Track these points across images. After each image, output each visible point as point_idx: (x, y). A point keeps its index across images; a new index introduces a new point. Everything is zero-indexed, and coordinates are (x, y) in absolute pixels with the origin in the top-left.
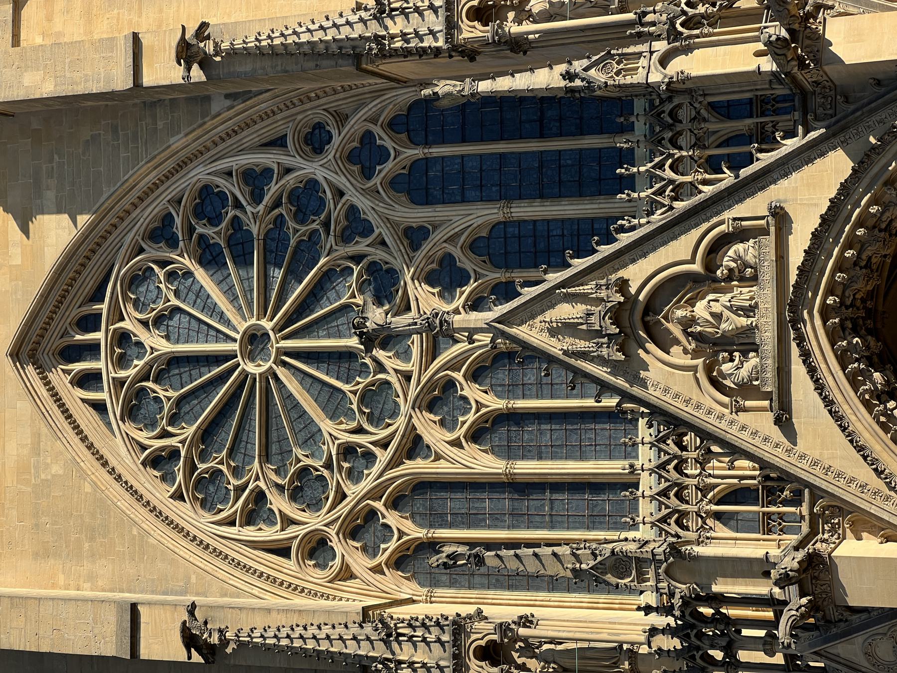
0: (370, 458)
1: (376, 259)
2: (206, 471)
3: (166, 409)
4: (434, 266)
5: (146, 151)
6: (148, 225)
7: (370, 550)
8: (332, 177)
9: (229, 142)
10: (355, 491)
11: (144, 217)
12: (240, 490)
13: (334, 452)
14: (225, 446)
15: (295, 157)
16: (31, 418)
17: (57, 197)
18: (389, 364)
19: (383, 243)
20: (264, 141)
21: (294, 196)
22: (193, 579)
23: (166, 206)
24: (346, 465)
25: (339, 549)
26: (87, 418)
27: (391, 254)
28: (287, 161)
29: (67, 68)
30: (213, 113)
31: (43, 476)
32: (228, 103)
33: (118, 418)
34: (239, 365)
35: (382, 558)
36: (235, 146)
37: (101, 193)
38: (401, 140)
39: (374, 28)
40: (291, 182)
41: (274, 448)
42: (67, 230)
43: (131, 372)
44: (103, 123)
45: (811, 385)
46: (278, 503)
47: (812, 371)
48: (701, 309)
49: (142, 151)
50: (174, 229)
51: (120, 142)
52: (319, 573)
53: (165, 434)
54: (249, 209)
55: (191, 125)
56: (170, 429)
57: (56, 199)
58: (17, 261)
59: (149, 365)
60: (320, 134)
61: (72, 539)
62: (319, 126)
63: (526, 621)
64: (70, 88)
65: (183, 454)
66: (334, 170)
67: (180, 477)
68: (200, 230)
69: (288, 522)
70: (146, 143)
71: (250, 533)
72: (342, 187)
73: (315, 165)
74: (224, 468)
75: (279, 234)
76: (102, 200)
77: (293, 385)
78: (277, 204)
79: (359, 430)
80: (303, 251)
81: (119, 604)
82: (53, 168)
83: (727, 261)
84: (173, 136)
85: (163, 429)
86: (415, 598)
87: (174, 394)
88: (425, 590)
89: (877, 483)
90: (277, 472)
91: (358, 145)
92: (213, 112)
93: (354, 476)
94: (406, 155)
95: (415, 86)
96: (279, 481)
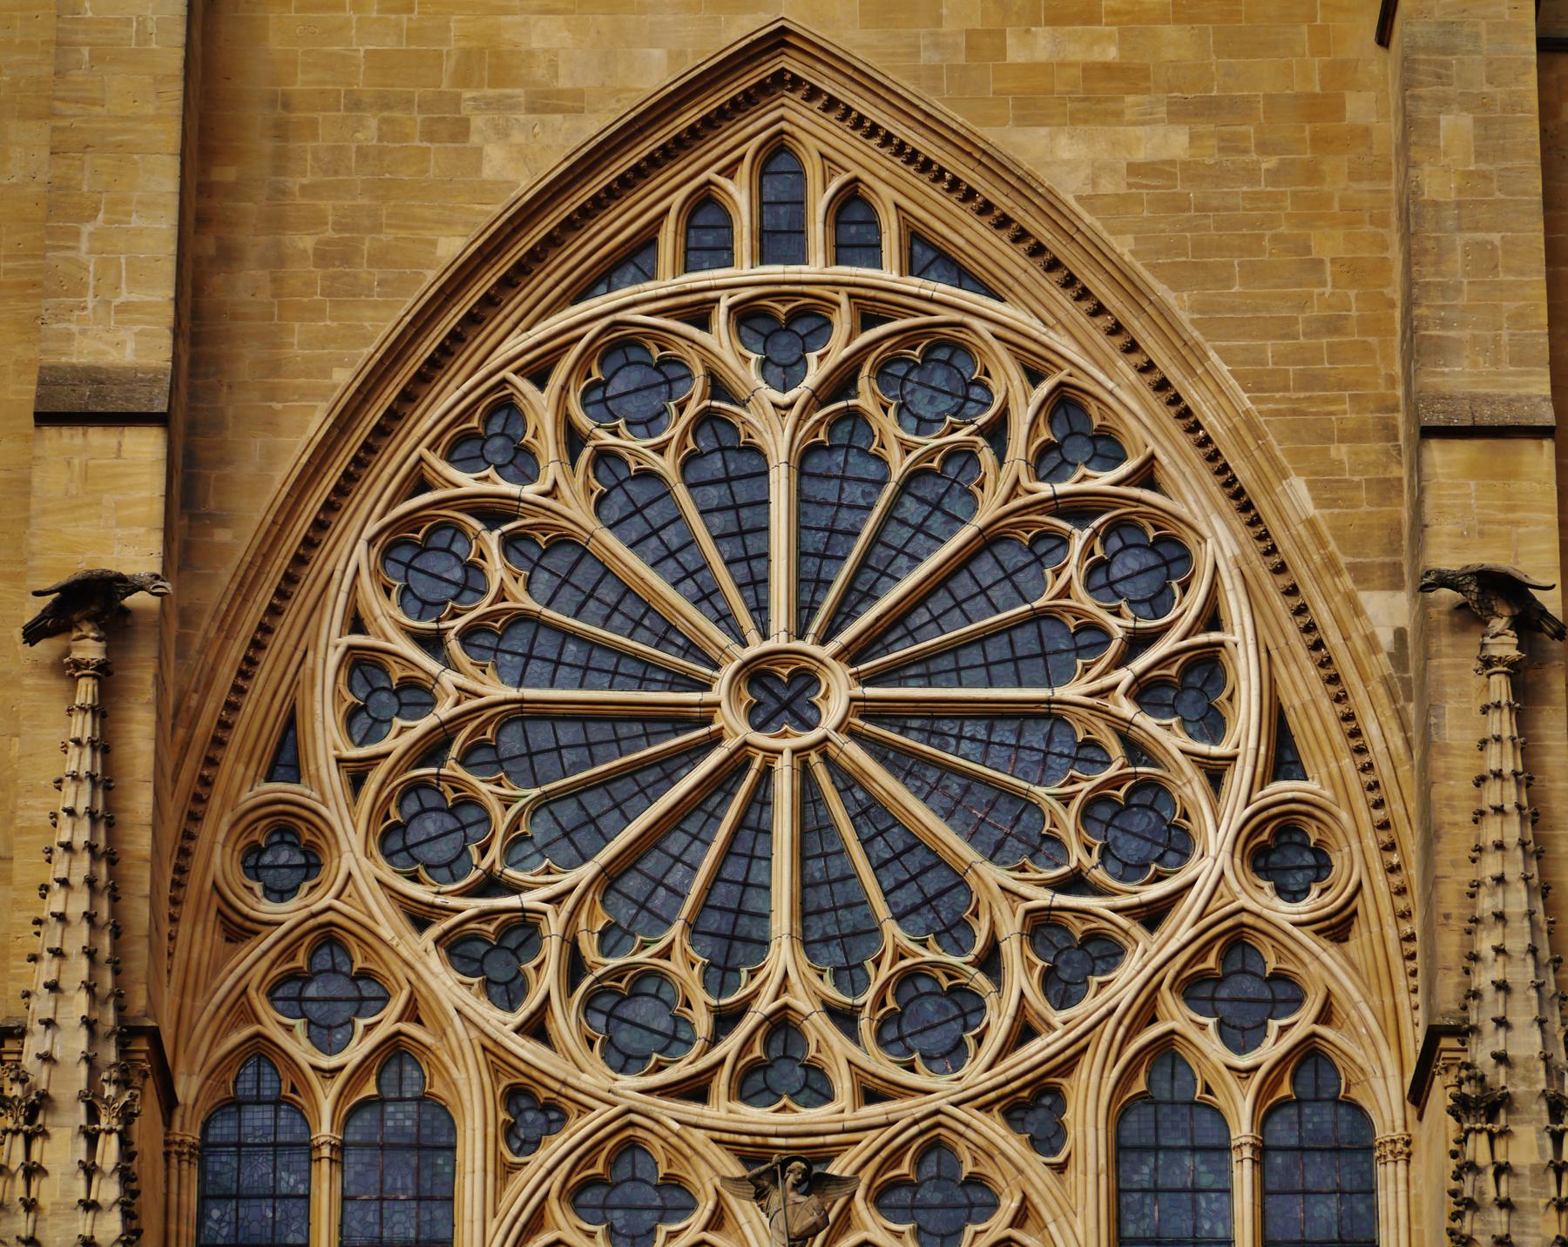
0: (508, 992)
1: (991, 1015)
4: (968, 1168)
5: (1278, 413)
6: (1097, 399)
8: (1192, 904)
9: (1291, 627)
11: (1117, 391)
13: (529, 900)
14: (548, 605)
15: (1248, 804)
16: (620, 91)
17: (1172, 163)
18: (731, 1043)
19: (1023, 1031)
20: (1292, 719)
21: (1152, 792)
22: (223, 535)
23: (1141, 446)
25: (289, 912)
26: (618, 225)
27: (1002, 1054)
28: (1239, 779)
29: (1479, 236)
30: (1363, 596)
31: (478, 121)
32: (1386, 638)
33: (619, 316)
34: (744, 644)
35: (271, 1023)
36: (1282, 642)
37: (1176, 286)
38: (1278, 1082)
40: (1188, 790)
41: (541, 735)
42: (1088, 190)
44: (1352, 293)
49: (1276, 401)
50: (1083, 470)
51: (1302, 340)
53: (573, 440)
54: (1124, 676)
55: (1336, 538)
56: (586, 453)
57: (1165, 162)
58: (1016, 53)
60: (1301, 868)
61: (322, 204)
62: (1322, 866)
64: (1430, 244)
65: (529, 492)
66: (1211, 907)
67: (467, 483)
68: (1079, 539)
70: (1294, 412)
72: (1168, 926)
73: (1224, 858)
75: (1061, 755)
76: (1161, 290)
78: (1136, 749)
79: (575, 967)
80: (1018, 819)
82: (1246, 151)
84: (1311, 485)
85: (589, 437)
86: (178, 1113)
91: (1269, 969)
92: (1363, 596)
94: (1238, 1097)
95: (1406, 1127)
96: (454, 751)
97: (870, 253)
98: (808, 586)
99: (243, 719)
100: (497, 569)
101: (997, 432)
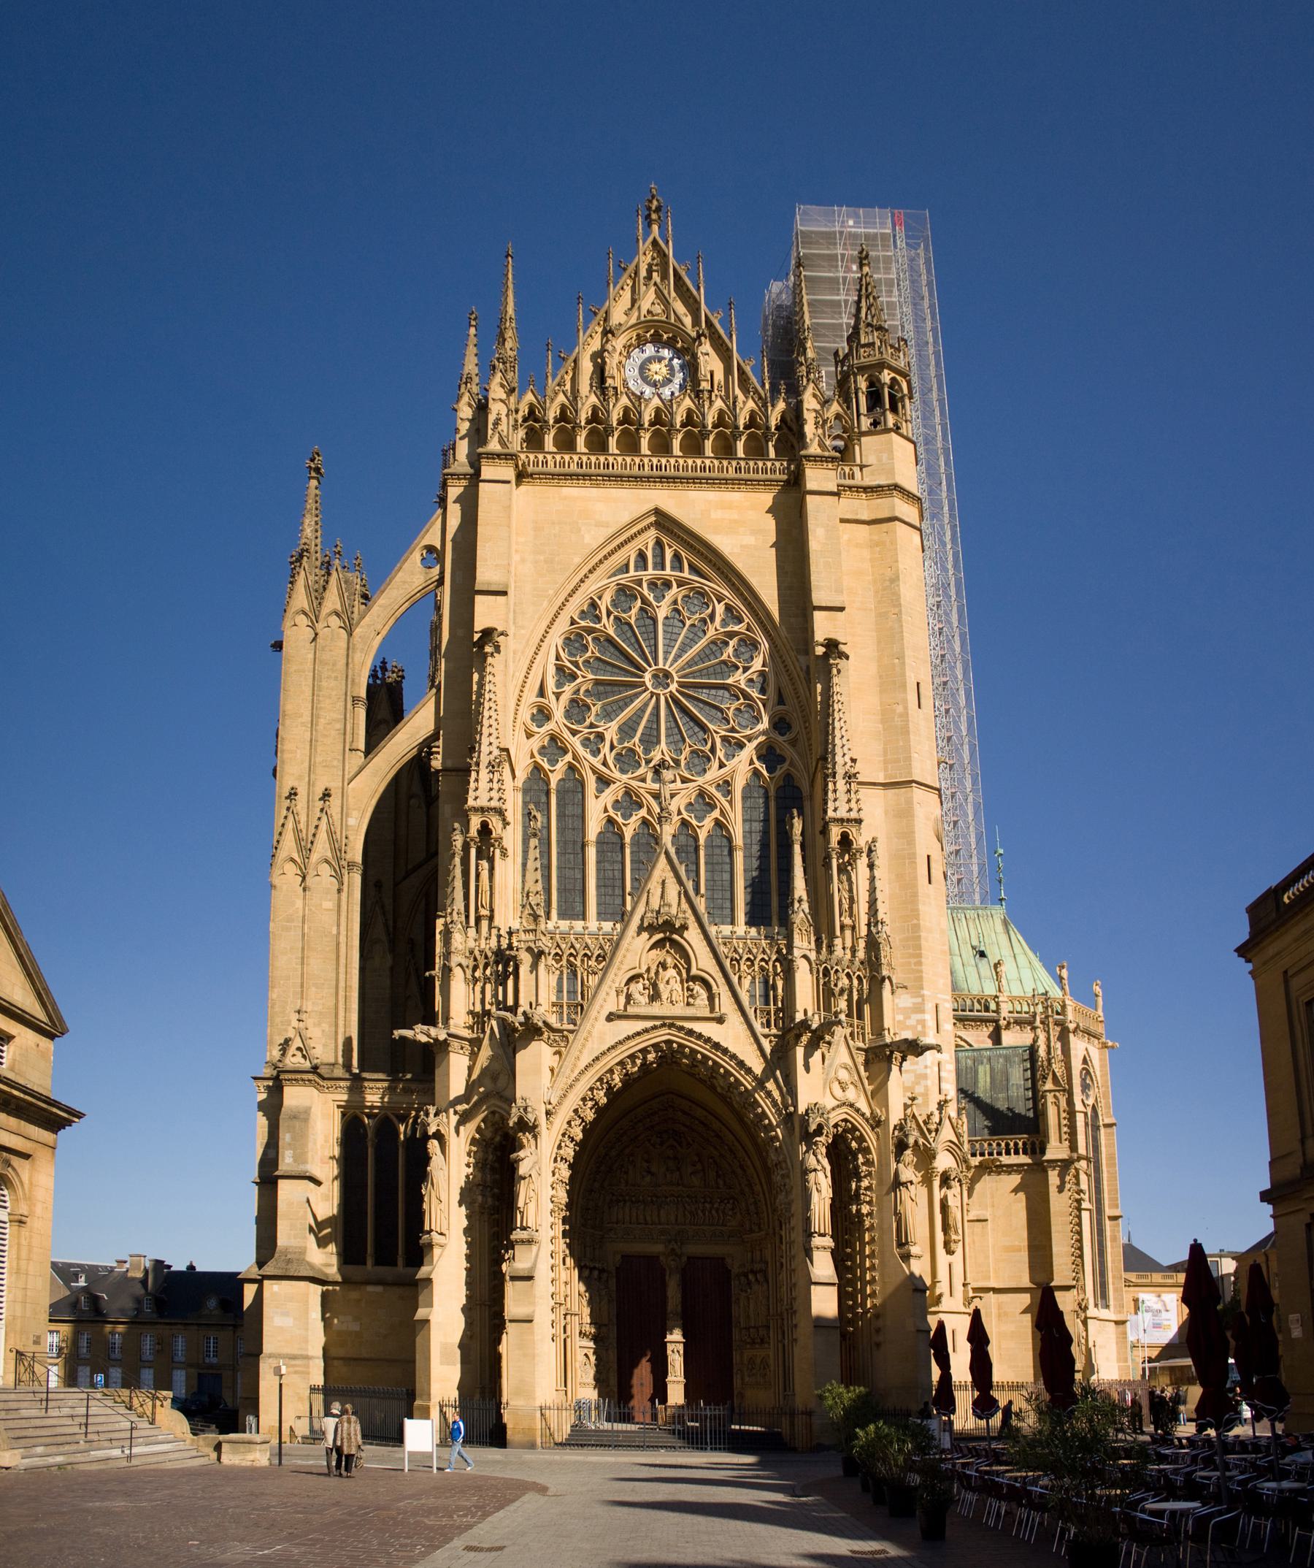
2: (587, 642)
3: (624, 615)
7: (542, 750)
10: (576, 742)
12: (577, 666)
13: (599, 730)
24: (592, 737)
25: (542, 730)
34: (650, 666)
35: (538, 758)
39: (840, 771)
41: (601, 688)
43: (646, 592)
45: (630, 1034)
46: (568, 689)
47: (638, 1034)
48: (671, 972)
52: (529, 717)
56: (612, 617)
59: (650, 605)
63: (504, 854)
65: (597, 626)
69: (558, 696)
71: (551, 670)
74: (589, 654)
77: (637, 703)
81: (507, 586)
83: (698, 988)
87: (633, 622)
88: (520, 785)
89: (582, 1065)
90: (587, 691)
93: (586, 742)
97: (681, 570)
98: (667, 653)
99: (529, 681)
100: (591, 646)
101: (712, 617)
